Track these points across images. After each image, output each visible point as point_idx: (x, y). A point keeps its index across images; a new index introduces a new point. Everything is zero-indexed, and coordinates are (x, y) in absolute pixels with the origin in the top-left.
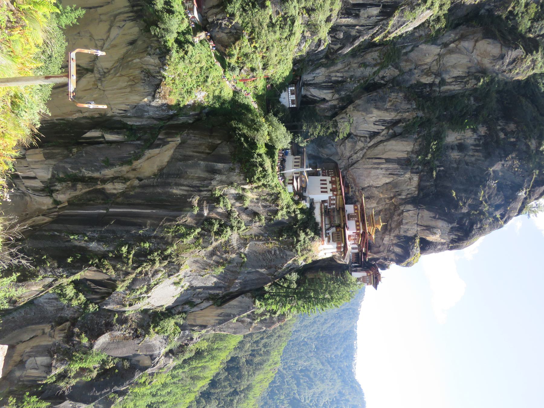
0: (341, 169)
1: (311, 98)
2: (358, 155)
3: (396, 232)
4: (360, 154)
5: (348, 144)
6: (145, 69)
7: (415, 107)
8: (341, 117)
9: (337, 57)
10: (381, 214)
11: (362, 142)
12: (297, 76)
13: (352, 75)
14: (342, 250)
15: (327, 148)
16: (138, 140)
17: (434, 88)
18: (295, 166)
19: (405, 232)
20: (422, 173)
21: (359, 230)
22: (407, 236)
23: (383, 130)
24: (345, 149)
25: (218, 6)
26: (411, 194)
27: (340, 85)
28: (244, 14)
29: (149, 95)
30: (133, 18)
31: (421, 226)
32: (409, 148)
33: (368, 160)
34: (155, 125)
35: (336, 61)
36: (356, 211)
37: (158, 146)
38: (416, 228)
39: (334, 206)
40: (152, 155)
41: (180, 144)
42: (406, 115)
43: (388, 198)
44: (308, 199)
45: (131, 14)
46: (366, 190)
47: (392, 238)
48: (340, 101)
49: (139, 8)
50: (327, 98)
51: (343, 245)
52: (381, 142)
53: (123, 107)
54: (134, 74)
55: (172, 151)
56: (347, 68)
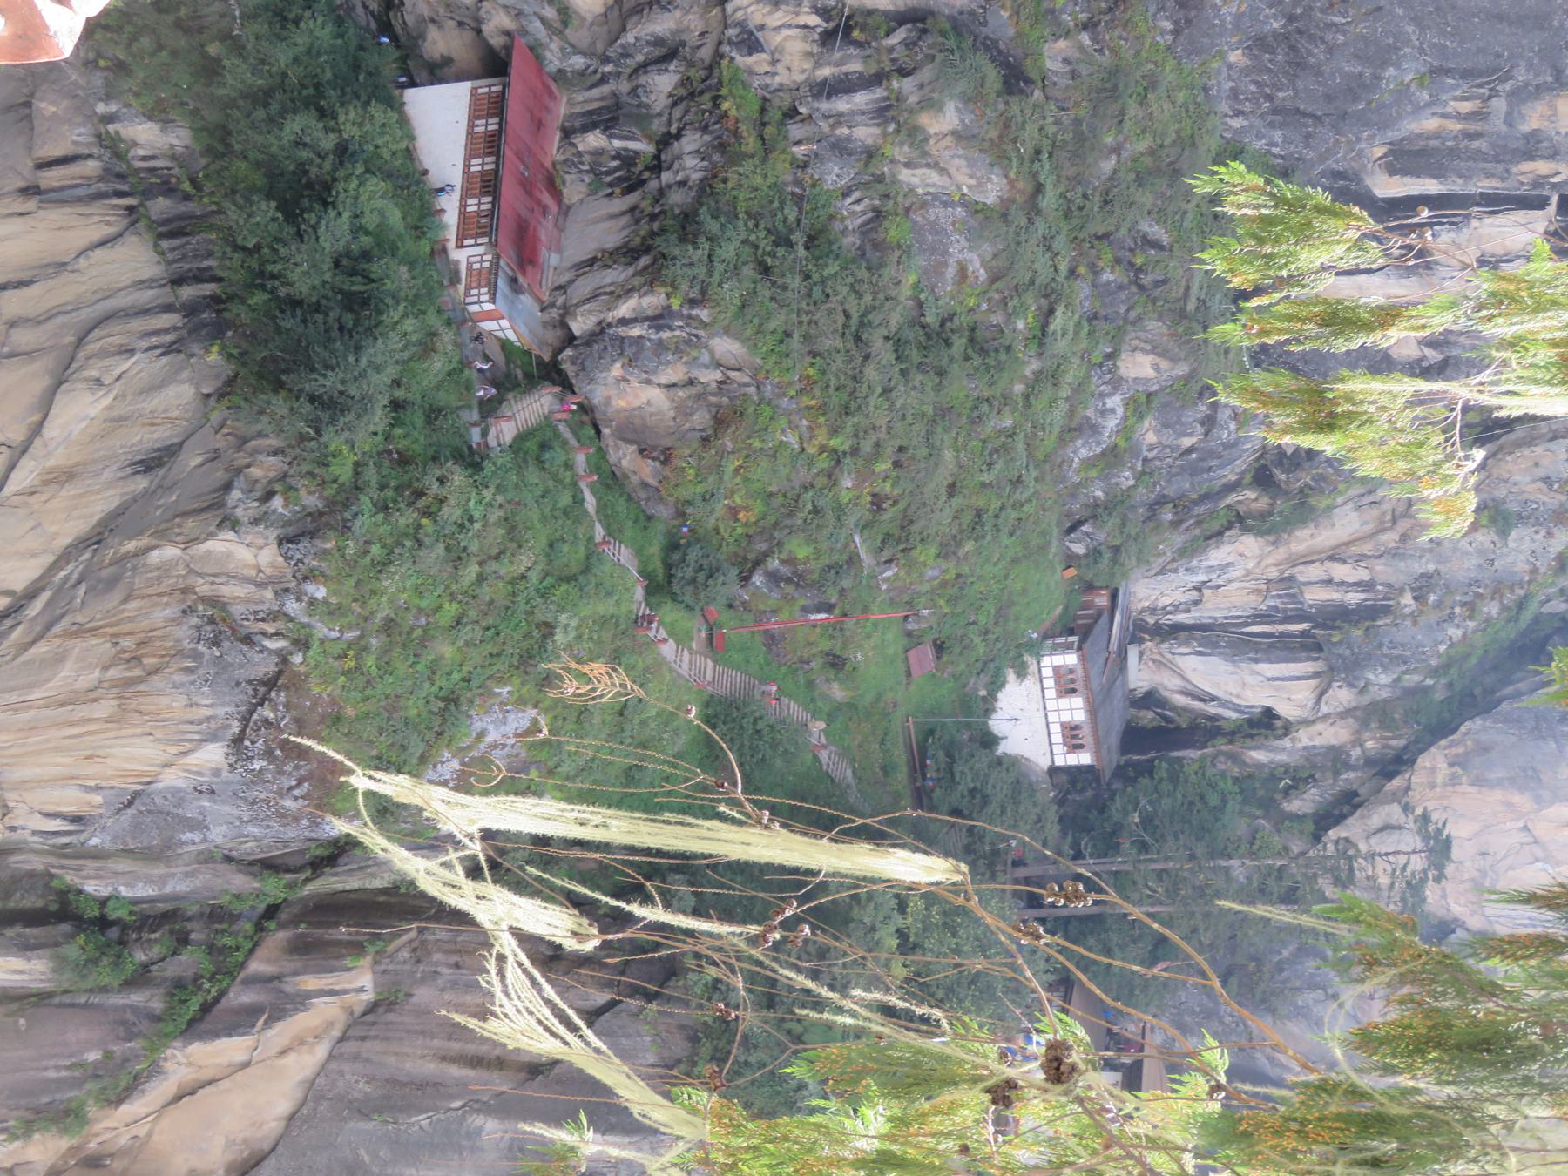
1: (1185, 709)
6: (202, 599)
8: (1376, 820)
9: (1322, 478)
12: (1090, 587)
15: (1302, 1013)
16: (129, 984)
25: (627, 253)
27: (1357, 633)
28: (765, 292)
29: (212, 737)
30: (169, 338)
34: (237, 896)
35: (1320, 502)
37: (244, 1020)
40: (206, 1075)
41: (373, 1008)
48: (1364, 724)
49: (209, 288)
50: (1285, 710)
53: (70, 799)
54: (145, 624)
55: (322, 1051)
56: (1390, 538)
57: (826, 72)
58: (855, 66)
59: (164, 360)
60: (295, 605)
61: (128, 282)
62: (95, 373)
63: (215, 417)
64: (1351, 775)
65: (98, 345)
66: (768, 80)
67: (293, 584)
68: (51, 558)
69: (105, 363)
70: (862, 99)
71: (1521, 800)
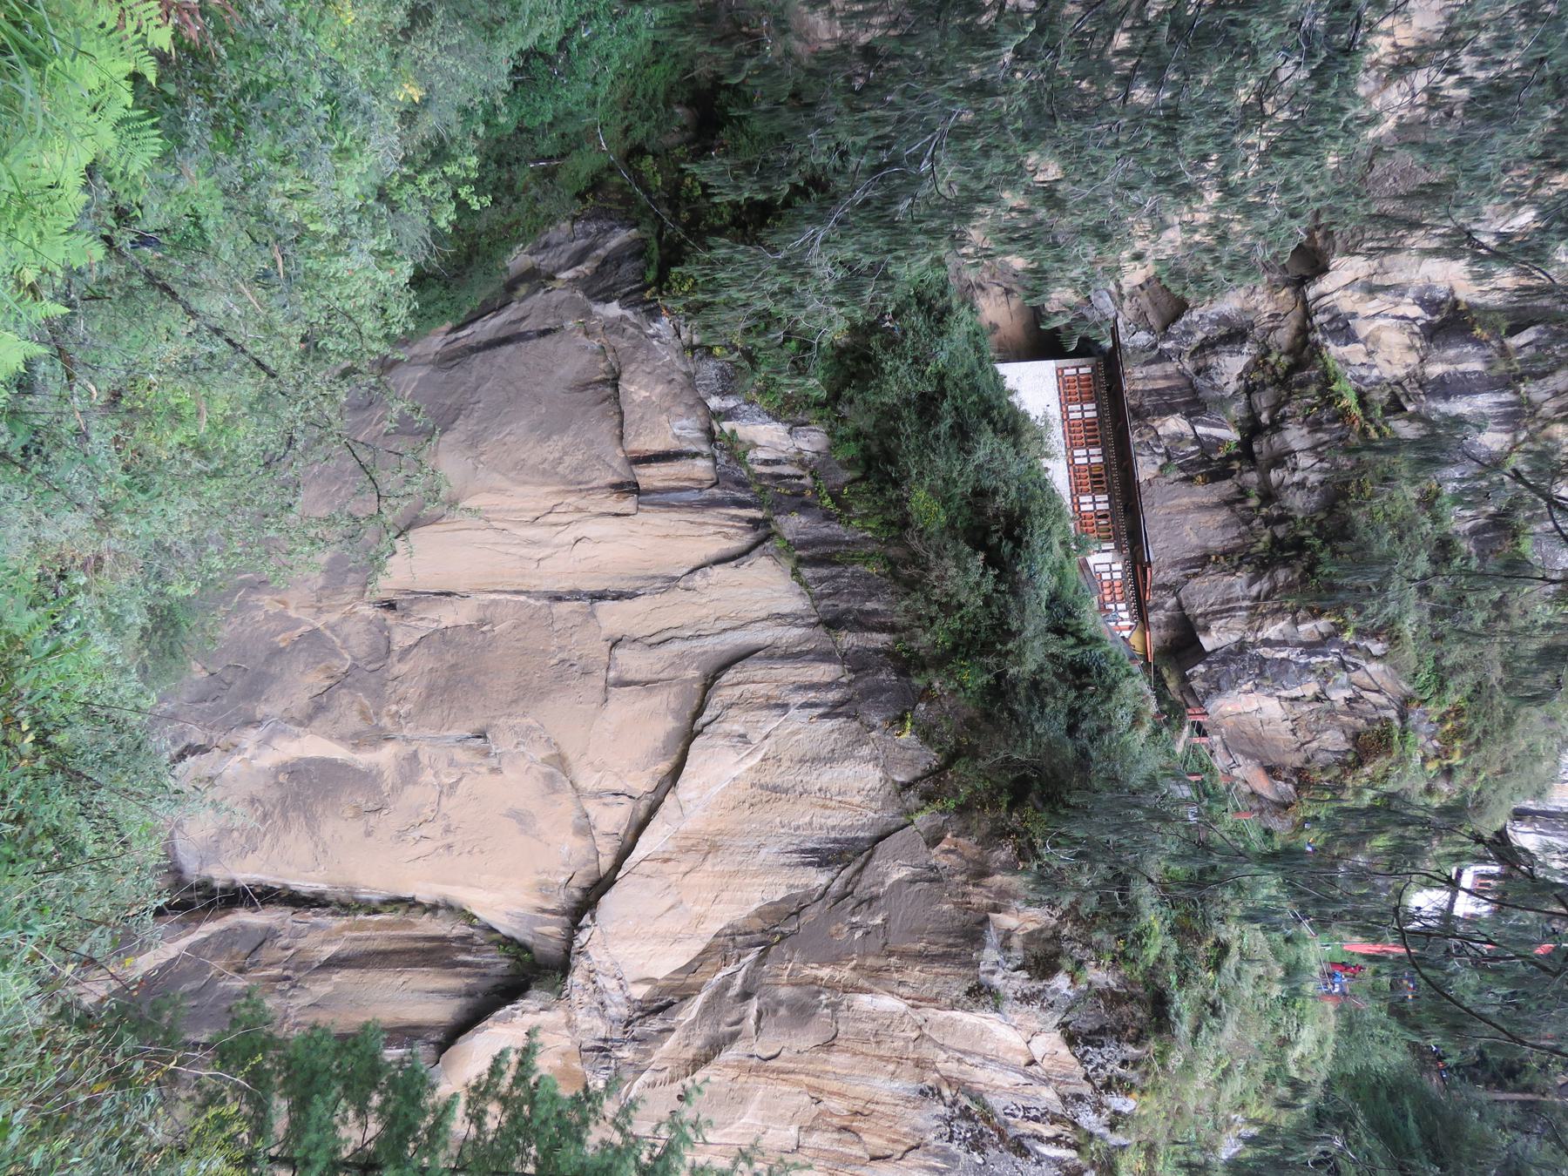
6: (949, 1081)
30: (833, 696)
45: (823, 672)
49: (880, 640)
54: (860, 1090)
57: (1435, 370)
58: (1475, 366)
59: (829, 724)
60: (1093, 1118)
61: (763, 614)
62: (738, 728)
63: (923, 820)
65: (737, 691)
66: (1364, 372)
67: (1087, 1089)
68: (697, 947)
69: (751, 716)
70: (1484, 402)
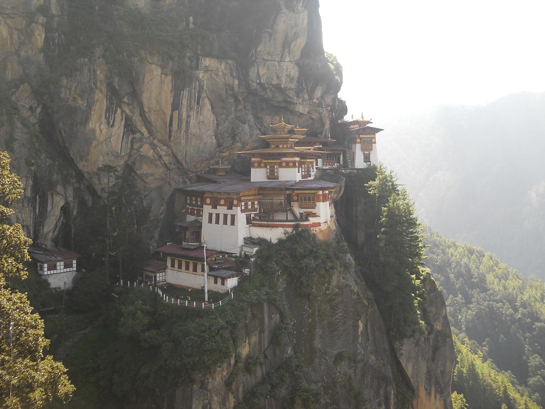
0: (185, 182)
2: (163, 153)
3: (292, 94)
4: (163, 150)
5: (144, 169)
7: (86, 60)
10: (260, 115)
11: (141, 147)
13: (26, 163)
14: (327, 192)
17: (55, 25)
18: (187, 268)
19: (291, 81)
20: (199, 52)
21: (294, 163)
22: (298, 78)
23: (123, 112)
24: (152, 175)
26: (231, 70)
31: (282, 55)
32: (157, 71)
33: (172, 138)
36: (263, 165)
38: (286, 64)
39: (256, 202)
42: (100, 75)
43: (236, 106)
44: (246, 249)
46: (221, 141)
47: (301, 100)
51: (321, 192)
52: (142, 114)
64: (82, 187)
71: (94, 143)
